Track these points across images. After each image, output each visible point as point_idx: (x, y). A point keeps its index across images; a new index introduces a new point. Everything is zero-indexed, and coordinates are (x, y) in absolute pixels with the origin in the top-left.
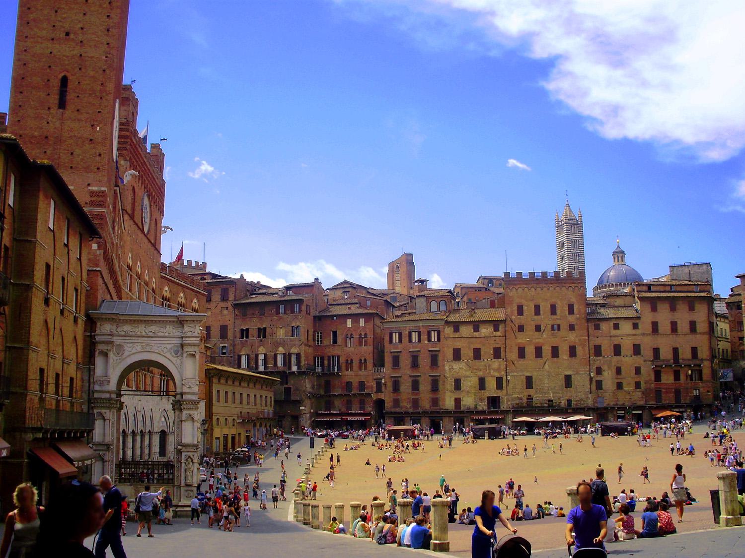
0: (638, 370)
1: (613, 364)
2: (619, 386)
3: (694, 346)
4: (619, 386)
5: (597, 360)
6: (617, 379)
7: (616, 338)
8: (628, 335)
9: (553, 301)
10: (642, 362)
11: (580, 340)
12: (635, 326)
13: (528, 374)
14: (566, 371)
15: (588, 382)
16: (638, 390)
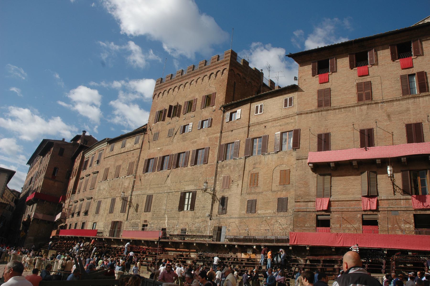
0: (285, 177)
1: (247, 168)
2: (252, 206)
3: (413, 120)
4: (252, 206)
5: (227, 165)
6: (249, 194)
7: (257, 127)
8: (275, 120)
9: (192, 95)
10: (293, 160)
11: (210, 140)
12: (289, 103)
13: (150, 192)
14: (188, 185)
15: (210, 201)
16: (282, 214)
